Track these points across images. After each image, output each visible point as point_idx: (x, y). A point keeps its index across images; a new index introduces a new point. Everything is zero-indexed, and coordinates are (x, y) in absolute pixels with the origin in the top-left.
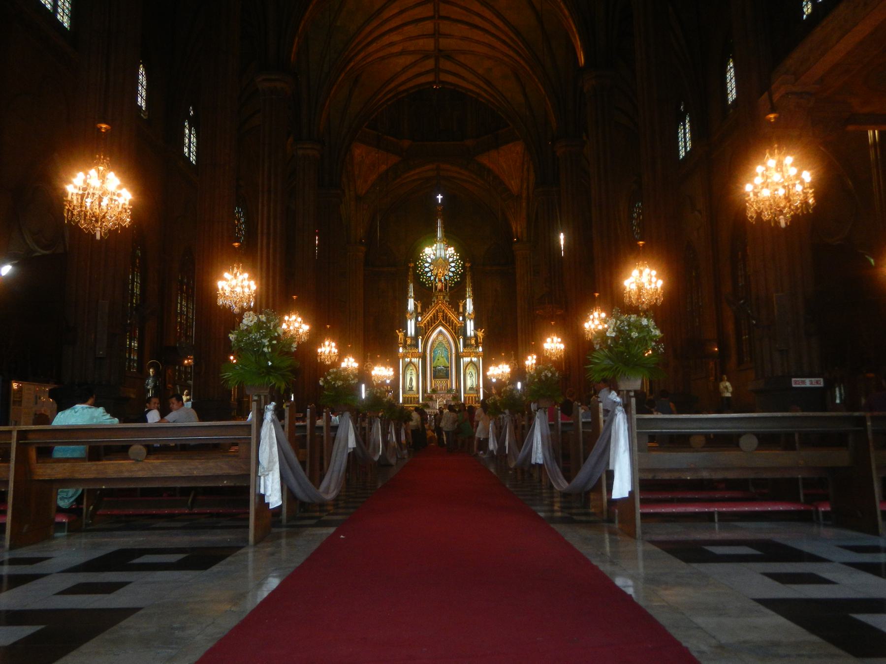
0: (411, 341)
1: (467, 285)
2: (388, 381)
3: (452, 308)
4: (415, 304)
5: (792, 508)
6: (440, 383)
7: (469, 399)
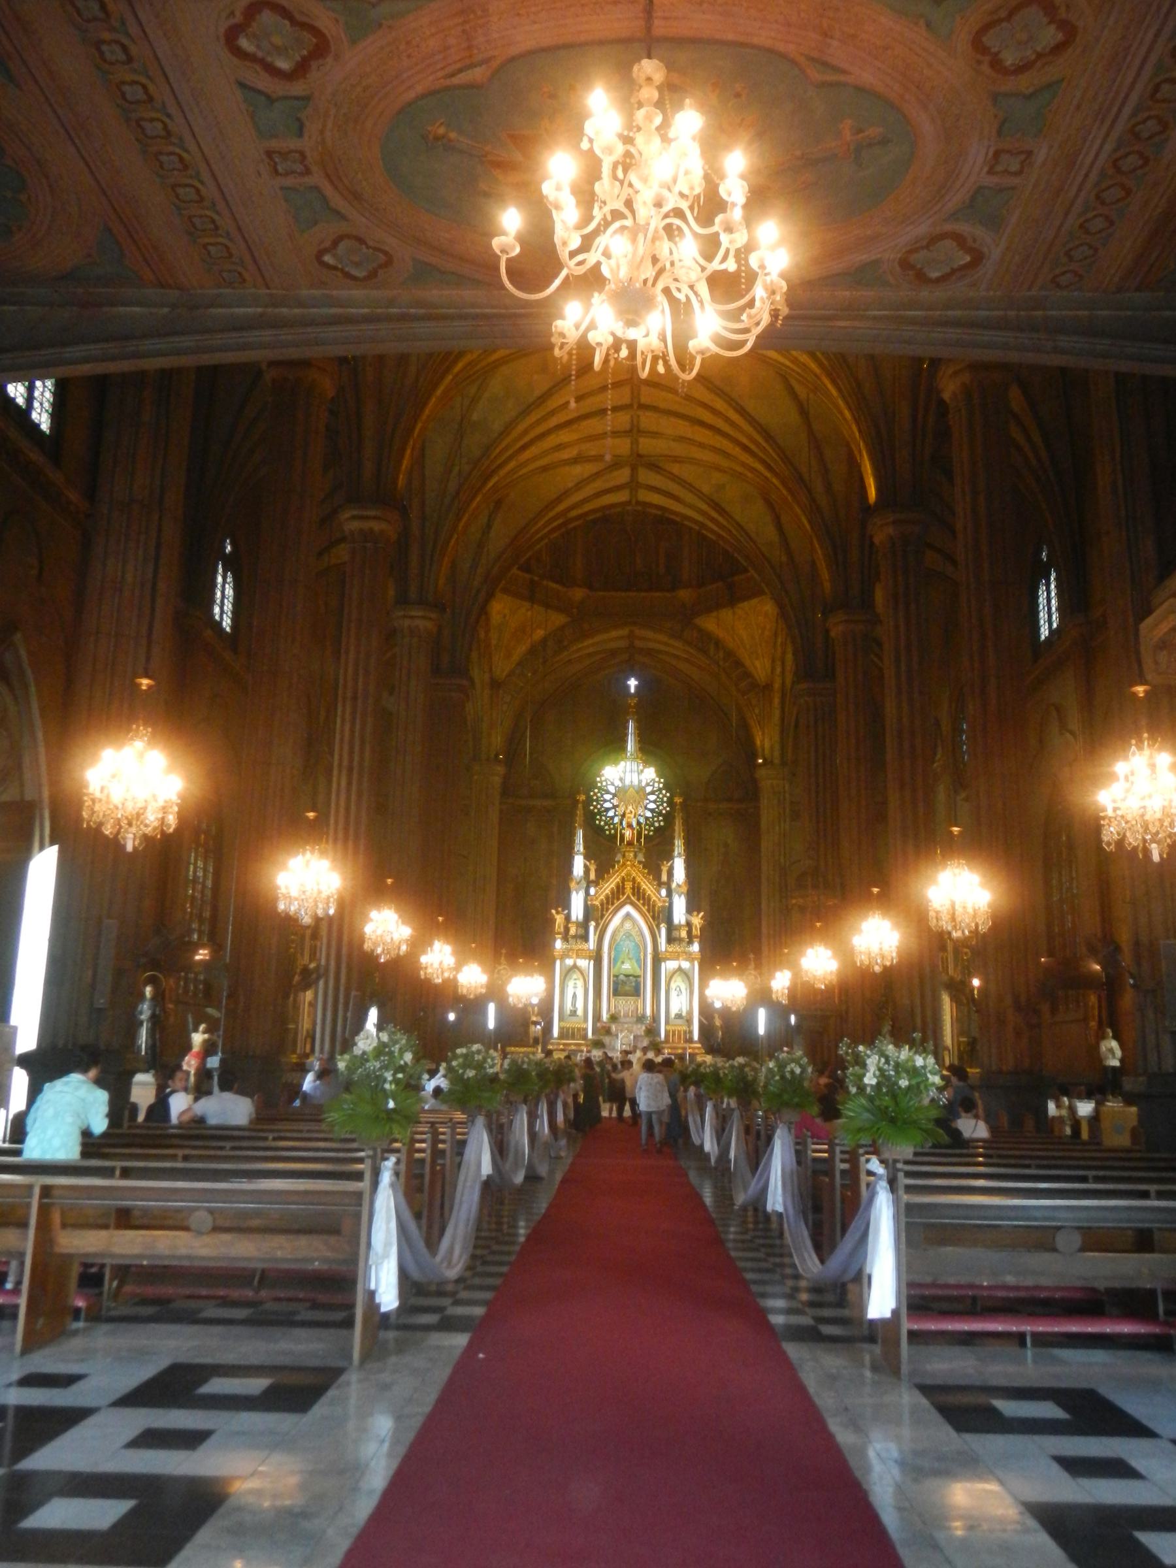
1: (676, 835)
2: (535, 1001)
3: (649, 874)
4: (586, 866)
5: (1143, 1331)
6: (625, 1005)
7: (674, 1034)
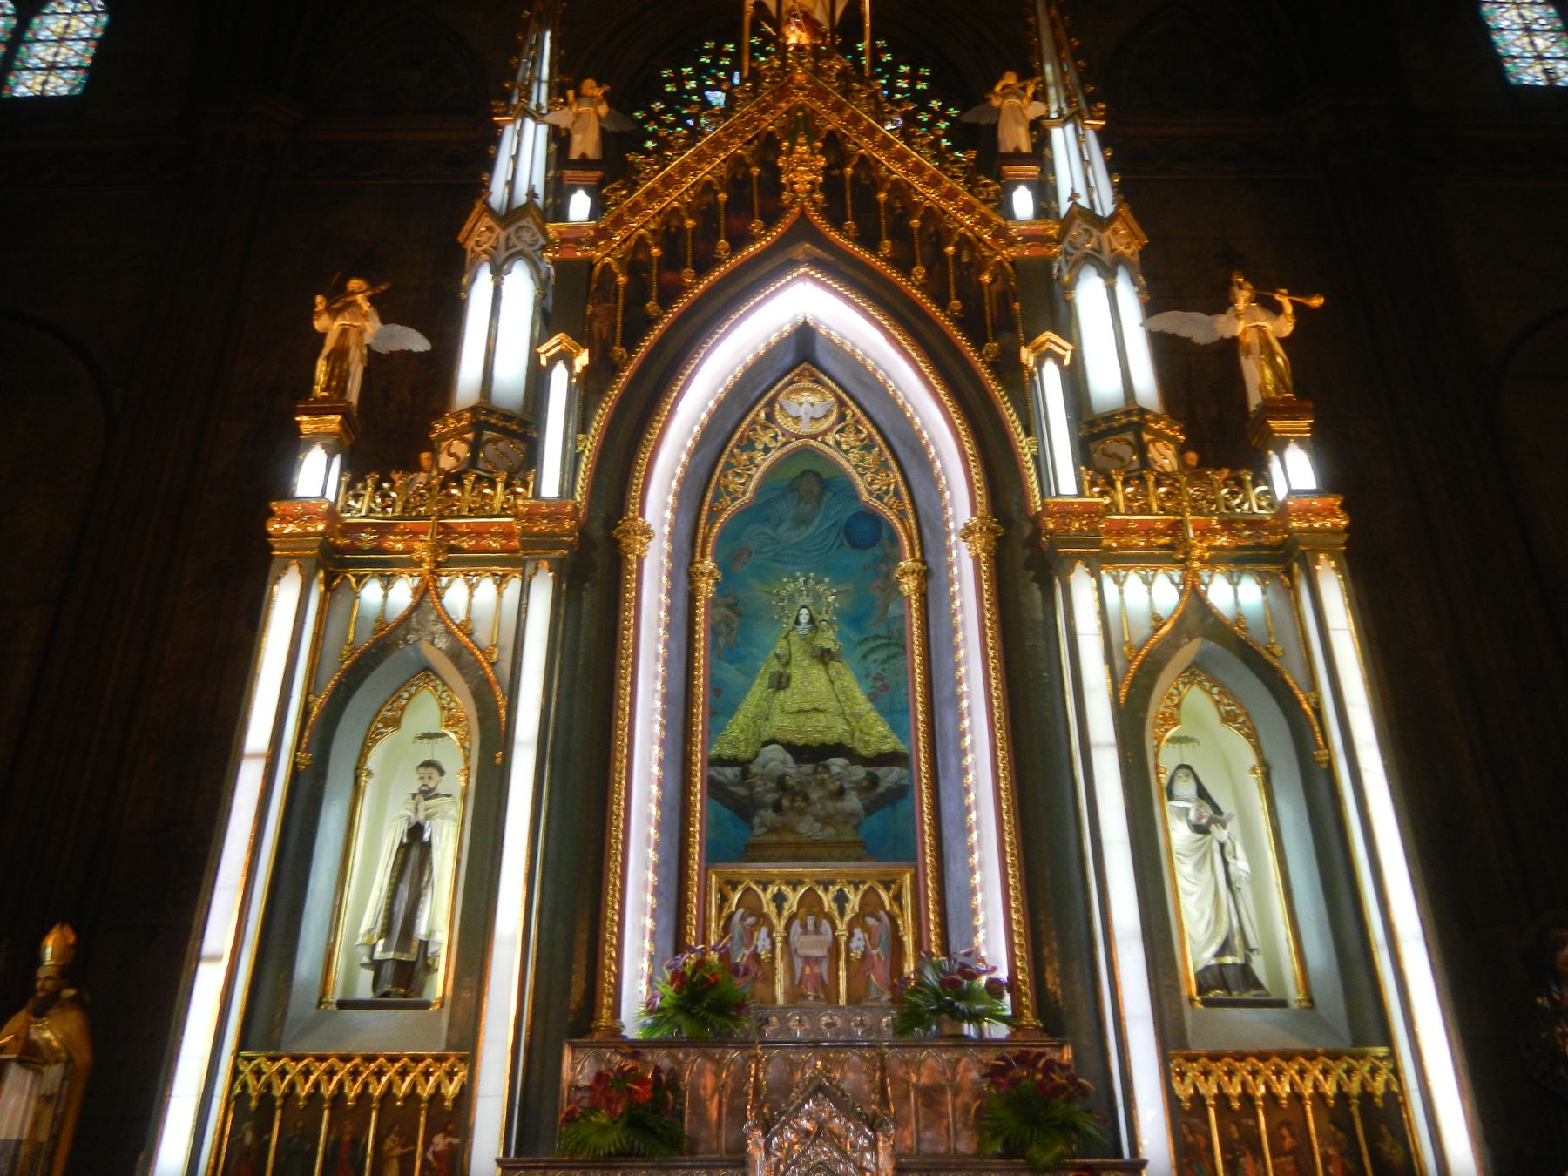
0: (475, 447)
7: (1242, 1144)
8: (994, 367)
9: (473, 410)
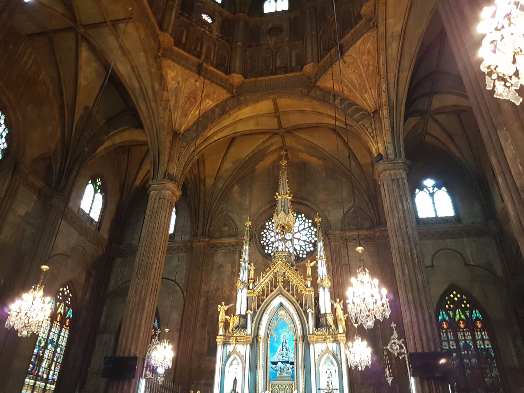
0: (239, 320)
8: (304, 312)
9: (239, 315)
